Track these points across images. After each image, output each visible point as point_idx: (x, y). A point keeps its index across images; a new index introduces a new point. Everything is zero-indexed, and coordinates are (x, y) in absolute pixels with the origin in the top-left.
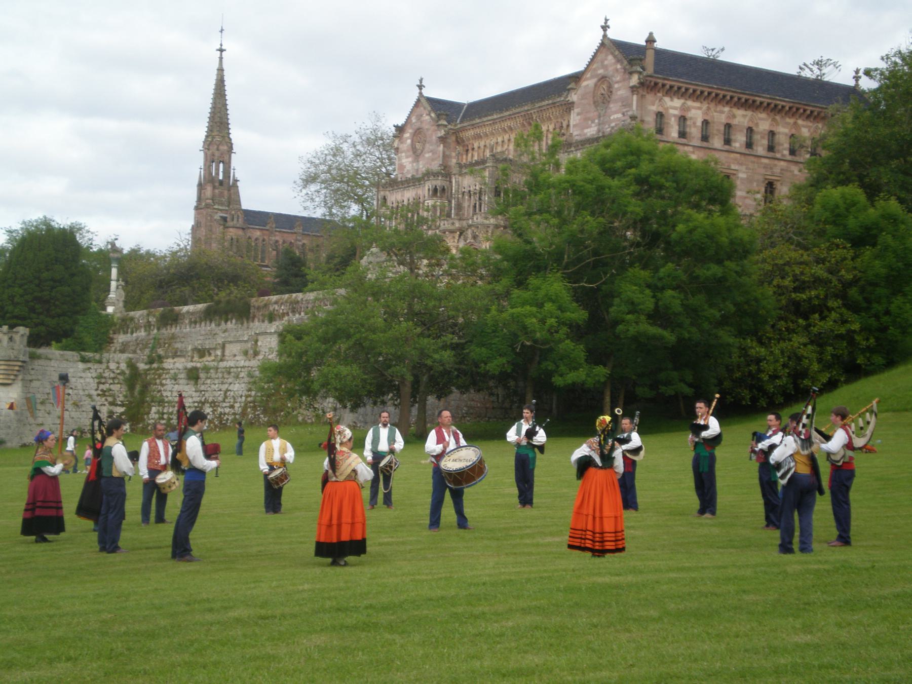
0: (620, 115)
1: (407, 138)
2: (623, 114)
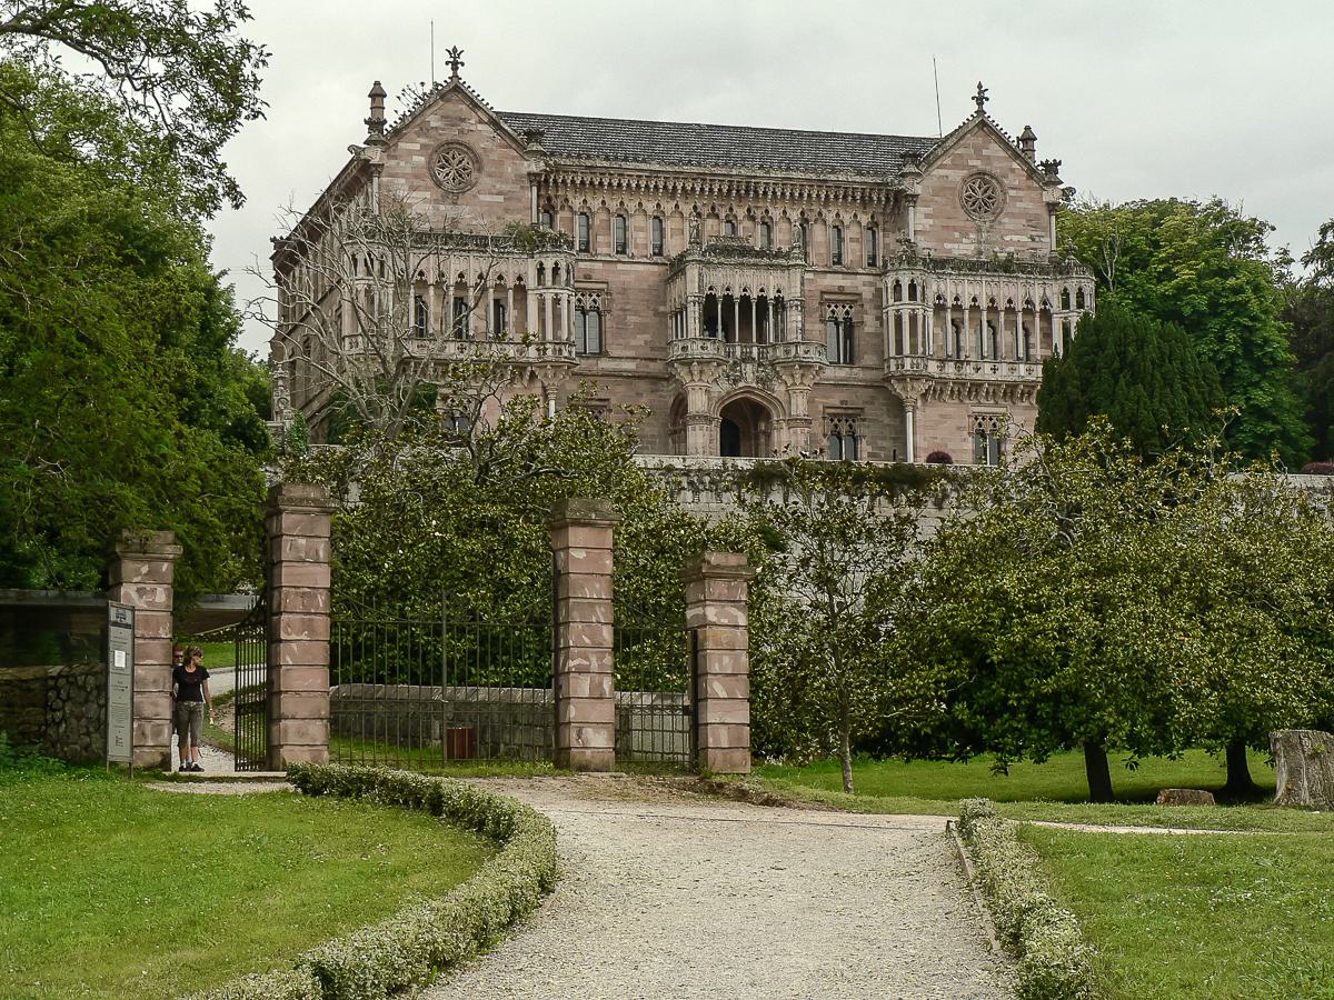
0: (1024, 239)
1: (411, 153)
2: (1033, 240)
